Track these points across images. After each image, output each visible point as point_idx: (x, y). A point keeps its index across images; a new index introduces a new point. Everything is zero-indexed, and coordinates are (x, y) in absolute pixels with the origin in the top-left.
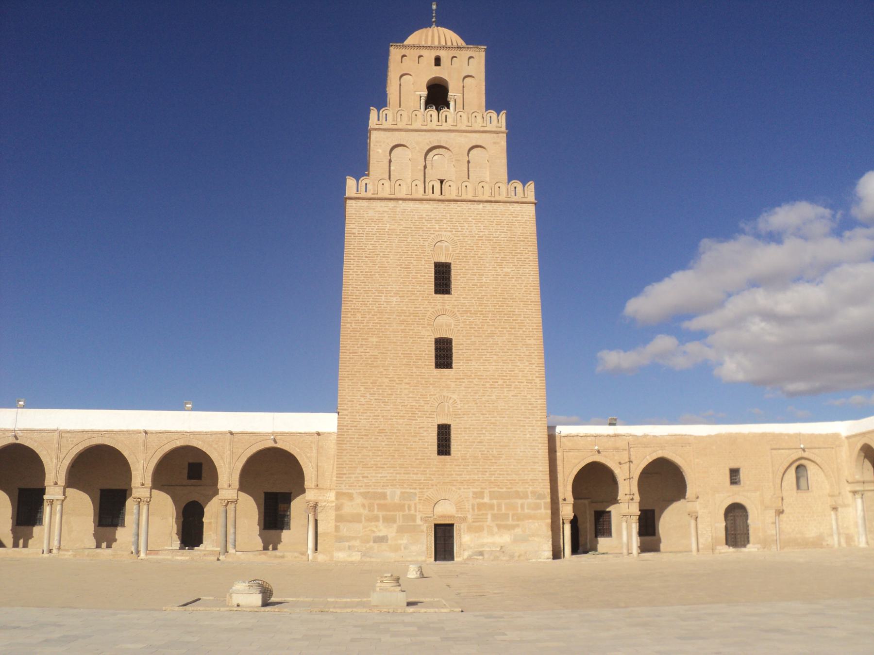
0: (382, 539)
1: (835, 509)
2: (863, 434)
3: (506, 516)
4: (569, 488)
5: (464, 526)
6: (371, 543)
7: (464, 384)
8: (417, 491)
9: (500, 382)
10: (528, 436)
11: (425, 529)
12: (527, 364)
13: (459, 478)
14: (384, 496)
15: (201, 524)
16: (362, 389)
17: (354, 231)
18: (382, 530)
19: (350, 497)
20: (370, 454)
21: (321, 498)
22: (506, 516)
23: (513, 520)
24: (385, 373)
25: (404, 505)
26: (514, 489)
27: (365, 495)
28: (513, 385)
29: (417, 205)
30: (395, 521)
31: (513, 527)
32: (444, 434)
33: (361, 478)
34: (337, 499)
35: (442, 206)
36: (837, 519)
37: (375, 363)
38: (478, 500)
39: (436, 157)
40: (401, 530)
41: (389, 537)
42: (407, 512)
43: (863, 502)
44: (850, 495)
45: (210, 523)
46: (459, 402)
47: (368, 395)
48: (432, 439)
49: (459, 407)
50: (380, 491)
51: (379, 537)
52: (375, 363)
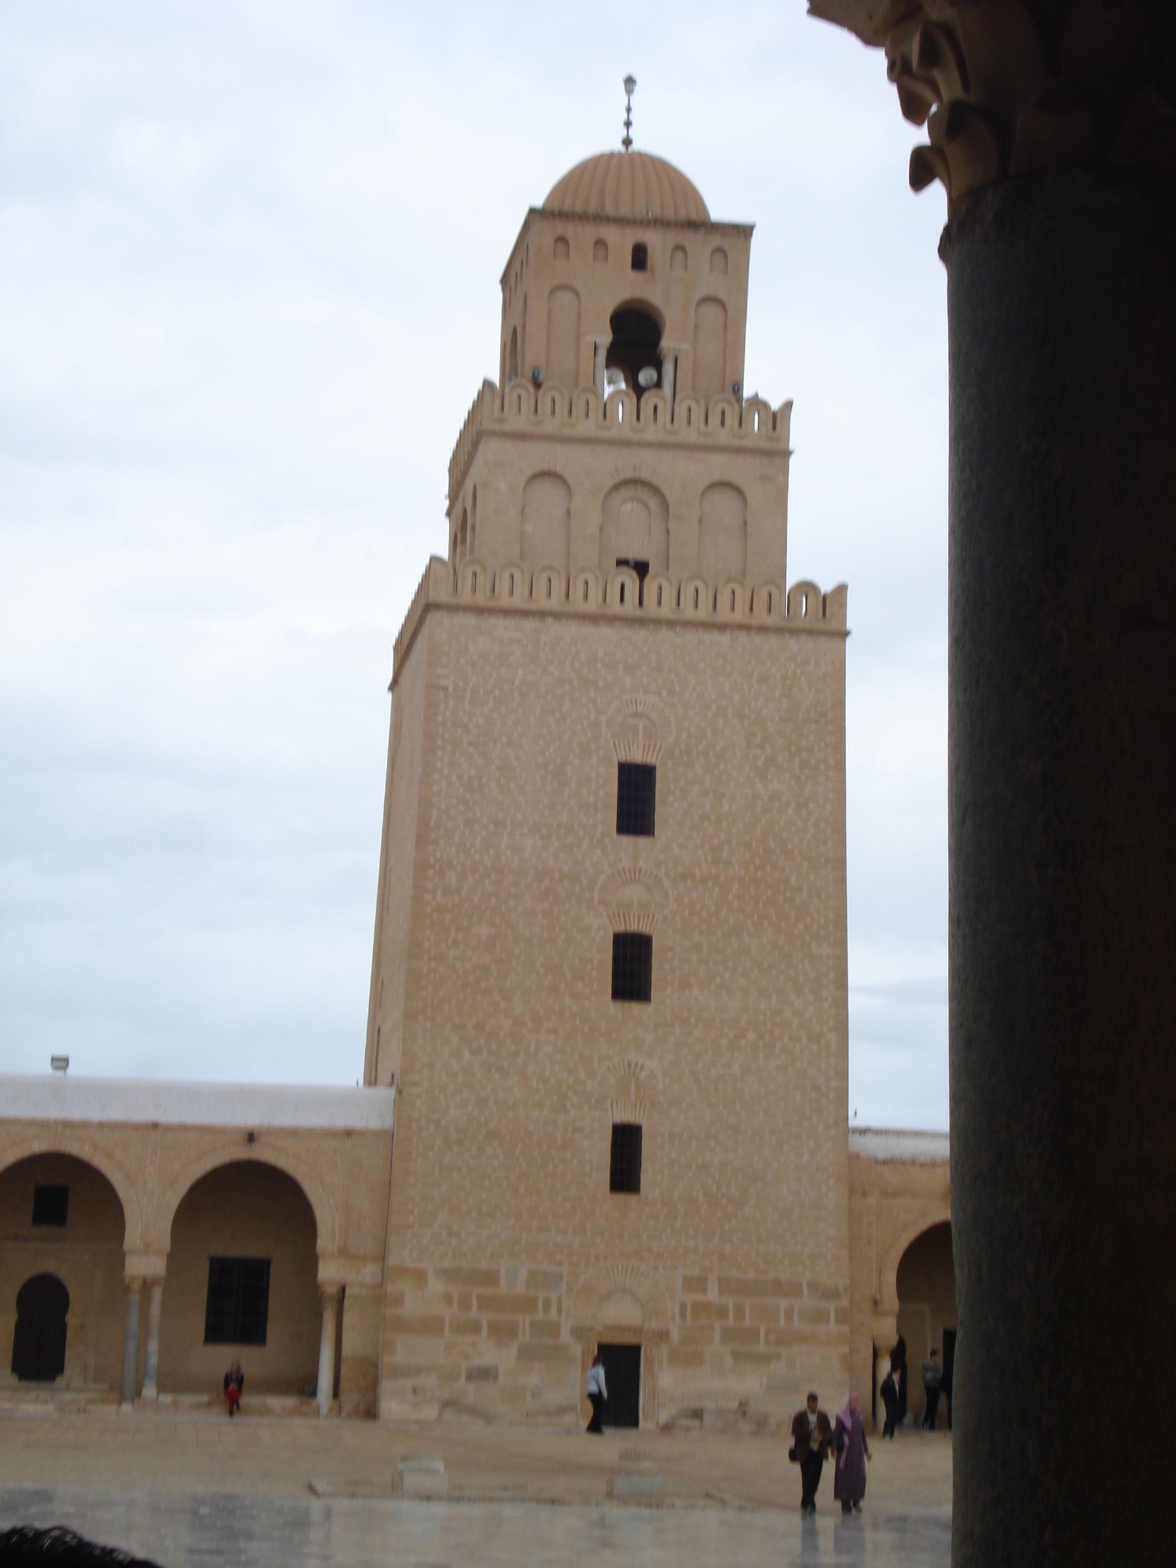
0: (484, 1374)
4: (891, 1277)
5: (665, 1350)
9: (751, 1036)
12: (811, 998)
14: (491, 1278)
15: (63, 1327)
17: (443, 682)
18: (486, 1352)
23: (767, 1342)
29: (587, 630)
32: (626, 1145)
35: (640, 635)
39: (628, 507)
40: (526, 1355)
42: (541, 1315)
45: (82, 1326)
47: (467, 1056)
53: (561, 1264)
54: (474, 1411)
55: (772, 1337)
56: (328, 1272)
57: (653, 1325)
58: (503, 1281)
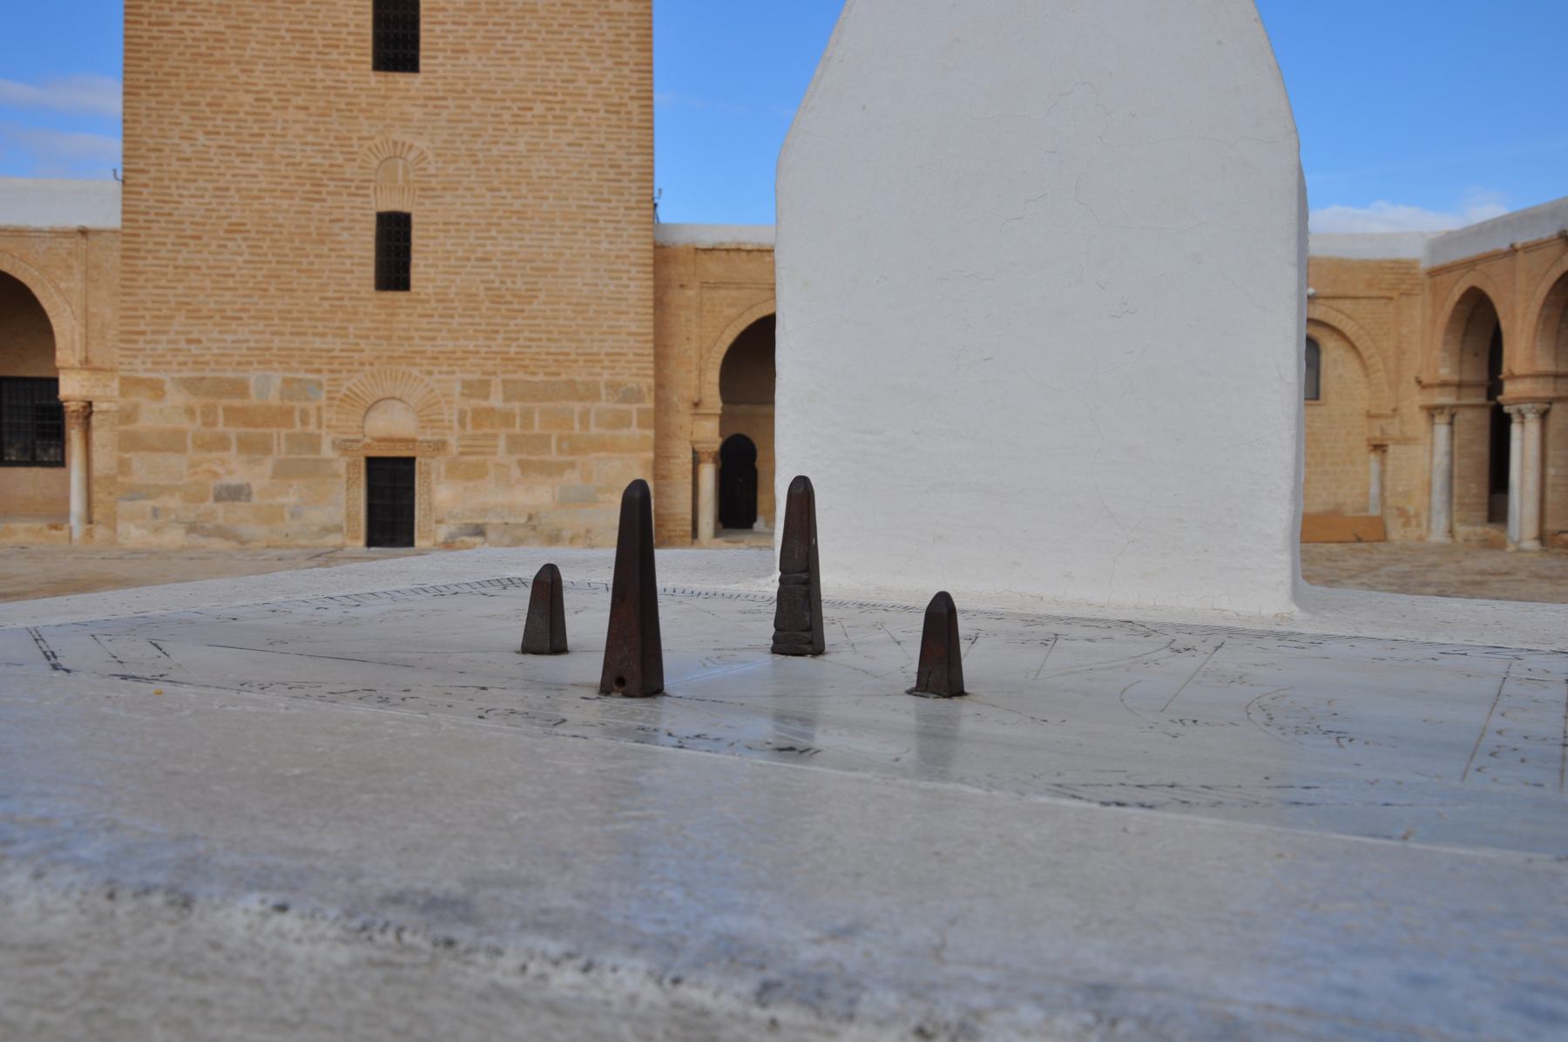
0: (236, 493)
1: (1379, 448)
2: (1471, 264)
3: (542, 442)
4: (713, 376)
6: (210, 503)
7: (445, 113)
8: (324, 377)
9: (539, 108)
10: (605, 245)
11: (342, 470)
12: (609, 63)
13: (428, 347)
14: (240, 388)
16: (185, 119)
18: (236, 470)
19: (157, 390)
20: (208, 284)
21: (98, 392)
22: (542, 442)
23: (560, 451)
24: (243, 78)
25: (290, 411)
26: (564, 377)
27: (191, 385)
28: (572, 117)
30: (265, 447)
31: (560, 468)
32: (394, 234)
33: (183, 345)
34: (123, 394)
36: (1383, 473)
37: (217, 54)
38: (475, 403)
40: (284, 472)
41: (255, 489)
42: (298, 428)
43: (1452, 433)
44: (1421, 418)
46: (431, 158)
47: (201, 138)
48: (363, 247)
49: (432, 171)
50: (230, 375)
51: (228, 488)
52: (217, 54)
53: (319, 371)
54: (222, 533)
55: (565, 446)
56: (71, 388)
57: (429, 436)
58: (252, 391)
